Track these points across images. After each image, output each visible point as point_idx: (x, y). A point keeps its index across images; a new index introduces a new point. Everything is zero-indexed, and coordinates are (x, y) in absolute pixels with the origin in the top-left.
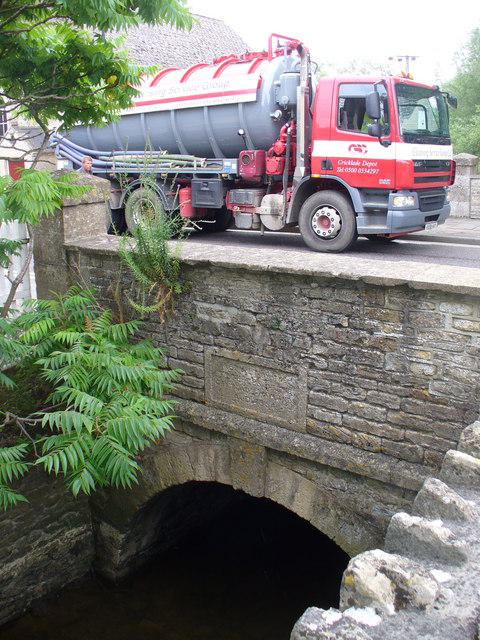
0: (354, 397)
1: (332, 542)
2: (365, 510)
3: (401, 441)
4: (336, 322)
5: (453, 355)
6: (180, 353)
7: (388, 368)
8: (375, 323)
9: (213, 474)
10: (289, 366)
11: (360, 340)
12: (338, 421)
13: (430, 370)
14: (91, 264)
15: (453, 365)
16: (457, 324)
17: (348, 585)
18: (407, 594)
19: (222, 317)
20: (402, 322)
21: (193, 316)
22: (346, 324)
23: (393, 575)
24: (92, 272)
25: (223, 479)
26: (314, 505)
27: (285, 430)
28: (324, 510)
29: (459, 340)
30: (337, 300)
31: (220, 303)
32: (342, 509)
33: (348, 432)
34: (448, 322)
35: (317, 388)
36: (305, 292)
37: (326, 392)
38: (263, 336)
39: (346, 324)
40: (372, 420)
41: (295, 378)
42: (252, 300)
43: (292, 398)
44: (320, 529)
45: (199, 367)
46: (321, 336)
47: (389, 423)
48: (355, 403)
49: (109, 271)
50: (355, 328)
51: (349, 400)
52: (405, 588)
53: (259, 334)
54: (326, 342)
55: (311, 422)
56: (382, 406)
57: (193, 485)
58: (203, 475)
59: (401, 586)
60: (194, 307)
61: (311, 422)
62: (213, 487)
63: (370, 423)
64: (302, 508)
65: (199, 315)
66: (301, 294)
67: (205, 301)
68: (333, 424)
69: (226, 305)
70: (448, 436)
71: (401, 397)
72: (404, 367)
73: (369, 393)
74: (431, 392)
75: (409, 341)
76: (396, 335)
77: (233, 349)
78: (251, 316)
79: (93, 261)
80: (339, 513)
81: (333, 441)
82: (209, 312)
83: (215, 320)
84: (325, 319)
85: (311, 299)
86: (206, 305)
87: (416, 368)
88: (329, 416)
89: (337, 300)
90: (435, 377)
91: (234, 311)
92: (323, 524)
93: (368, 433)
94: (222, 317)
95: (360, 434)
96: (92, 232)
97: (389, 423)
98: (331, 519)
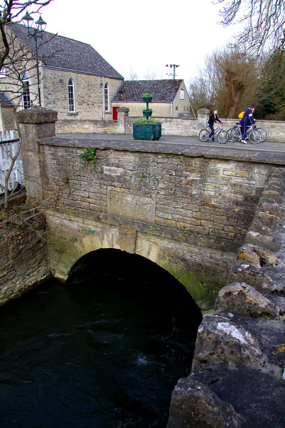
0: (178, 207)
1: (167, 272)
2: (182, 257)
3: (199, 225)
4: (170, 173)
5: (223, 187)
6: (95, 190)
7: (193, 193)
8: (188, 173)
9: (111, 245)
10: (148, 194)
11: (181, 181)
12: (170, 218)
13: (213, 193)
14: (51, 150)
15: (223, 191)
16: (225, 173)
17: (241, 258)
18: (265, 260)
19: (116, 173)
20: (200, 172)
21: (102, 172)
22: (174, 174)
23: (259, 253)
24: (51, 154)
25: (117, 247)
26: (159, 256)
27: (145, 223)
28: (164, 257)
29: (226, 180)
30: (170, 164)
31: (115, 166)
32: (172, 257)
33: (174, 222)
34: (221, 172)
35: (160, 203)
36: (156, 160)
37: (164, 205)
38: (135, 181)
39: (174, 174)
40: (185, 217)
41: (150, 199)
42: (130, 164)
43: (149, 208)
44: (161, 266)
45: (104, 196)
46: (163, 180)
47: (194, 218)
48: (178, 209)
49: (60, 153)
50: (179, 176)
51: (175, 208)
52: (264, 258)
53: (133, 180)
54: (165, 182)
55: (157, 219)
56: (190, 210)
57: (102, 250)
58: (106, 246)
59: (262, 257)
60: (102, 169)
61: (157, 219)
62: (112, 251)
63: (185, 218)
64: (153, 257)
65: (105, 172)
66: (153, 161)
67: (108, 165)
68: (168, 219)
69: (117, 167)
70: (220, 222)
71: (199, 206)
72: (201, 193)
73: (185, 204)
74: (213, 203)
75: (203, 181)
76: (197, 179)
77: (121, 188)
78: (129, 171)
79: (52, 149)
80: (170, 258)
81: (167, 227)
82: (110, 170)
83: (112, 174)
84: (164, 172)
85: (157, 163)
86: (108, 168)
87: (206, 193)
88: (166, 216)
89: (170, 164)
90: (215, 196)
91: (121, 170)
92: (162, 264)
93: (184, 223)
94: (116, 173)
95: (180, 223)
96: (50, 136)
97: (194, 218)
98: (166, 262)
